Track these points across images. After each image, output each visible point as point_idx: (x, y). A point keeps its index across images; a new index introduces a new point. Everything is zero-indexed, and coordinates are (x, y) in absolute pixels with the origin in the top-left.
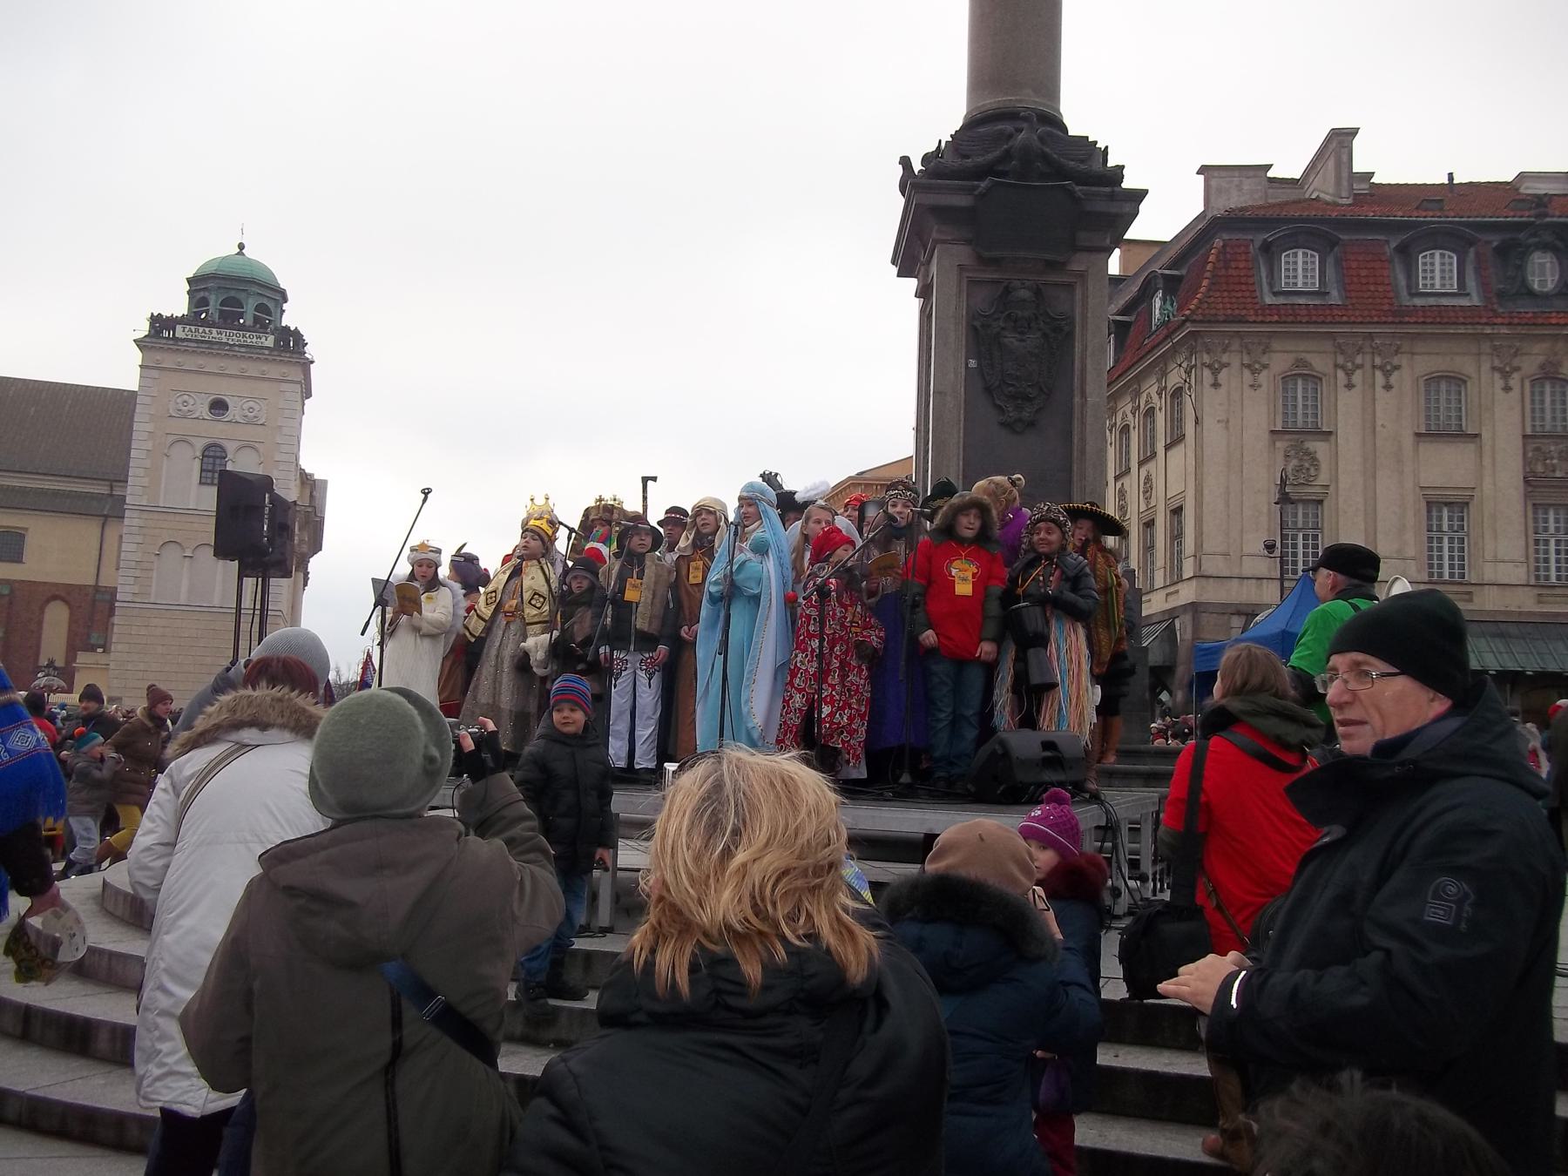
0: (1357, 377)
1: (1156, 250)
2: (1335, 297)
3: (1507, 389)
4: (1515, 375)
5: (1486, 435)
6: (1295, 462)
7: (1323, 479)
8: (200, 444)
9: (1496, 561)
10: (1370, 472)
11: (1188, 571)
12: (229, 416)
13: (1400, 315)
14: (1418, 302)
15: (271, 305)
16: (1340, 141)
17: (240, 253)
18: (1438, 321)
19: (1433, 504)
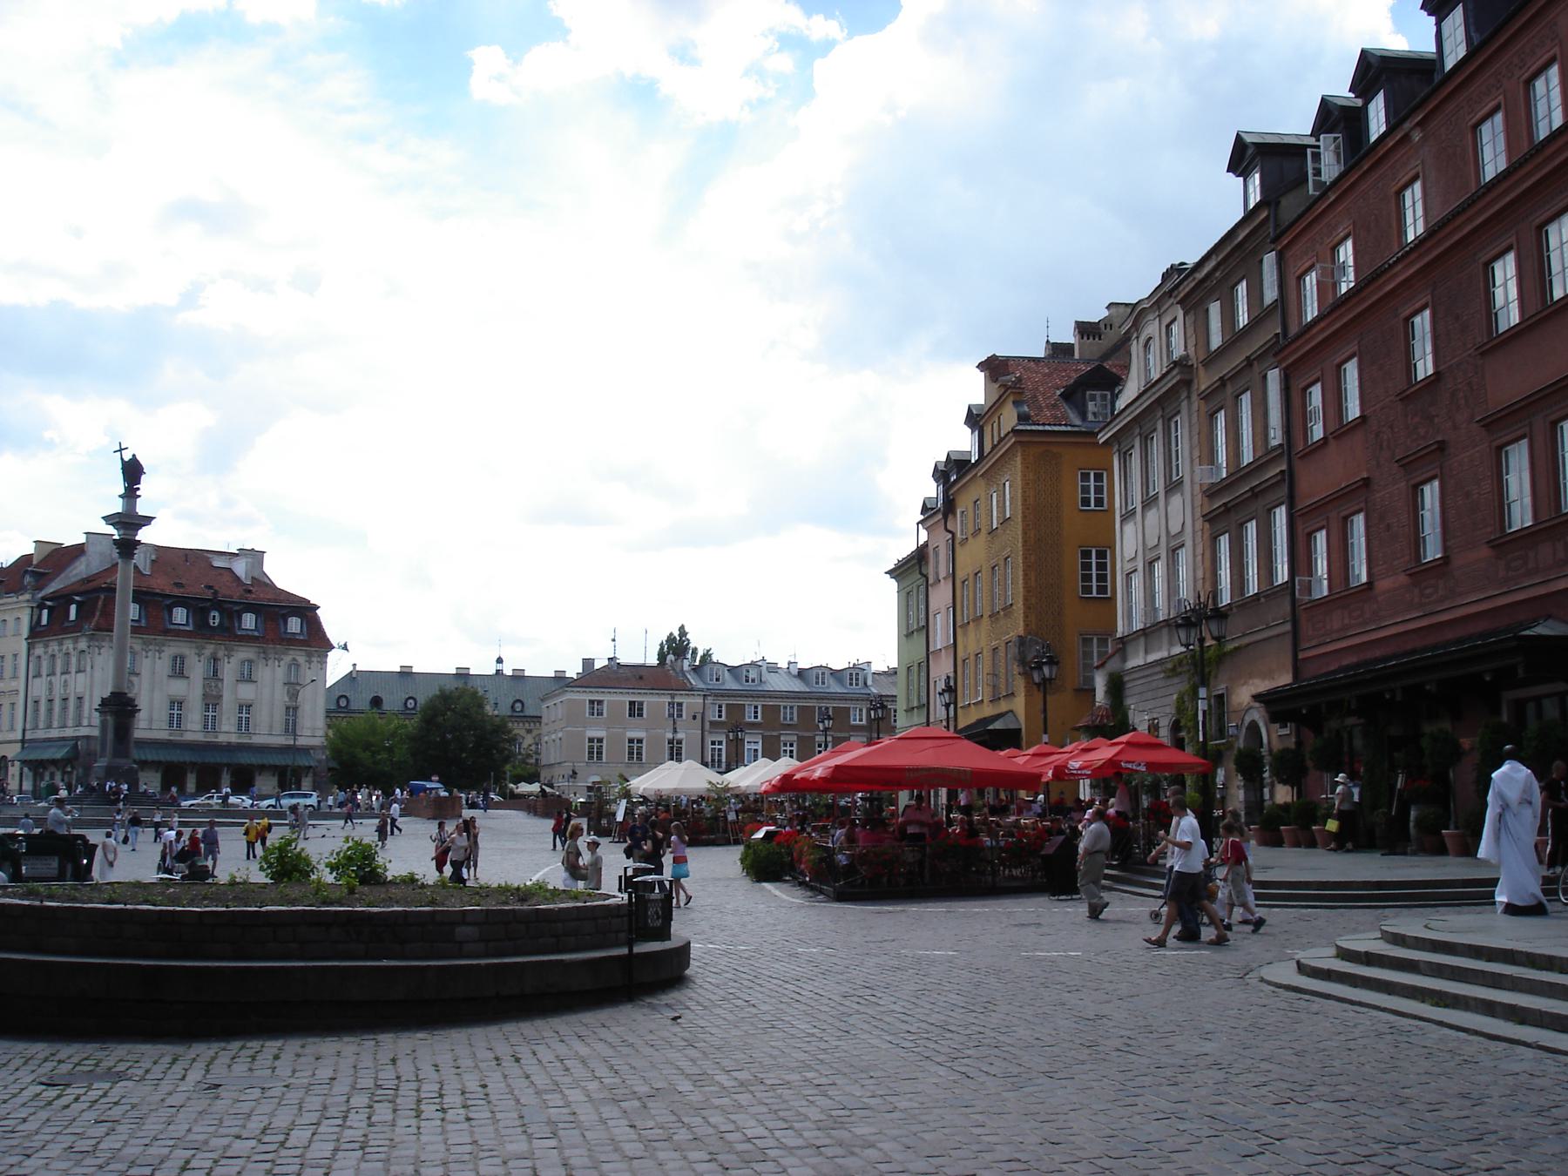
2: (143, 623)
10: (152, 690)
11: (85, 722)
13: (166, 632)
18: (178, 634)
19: (172, 703)
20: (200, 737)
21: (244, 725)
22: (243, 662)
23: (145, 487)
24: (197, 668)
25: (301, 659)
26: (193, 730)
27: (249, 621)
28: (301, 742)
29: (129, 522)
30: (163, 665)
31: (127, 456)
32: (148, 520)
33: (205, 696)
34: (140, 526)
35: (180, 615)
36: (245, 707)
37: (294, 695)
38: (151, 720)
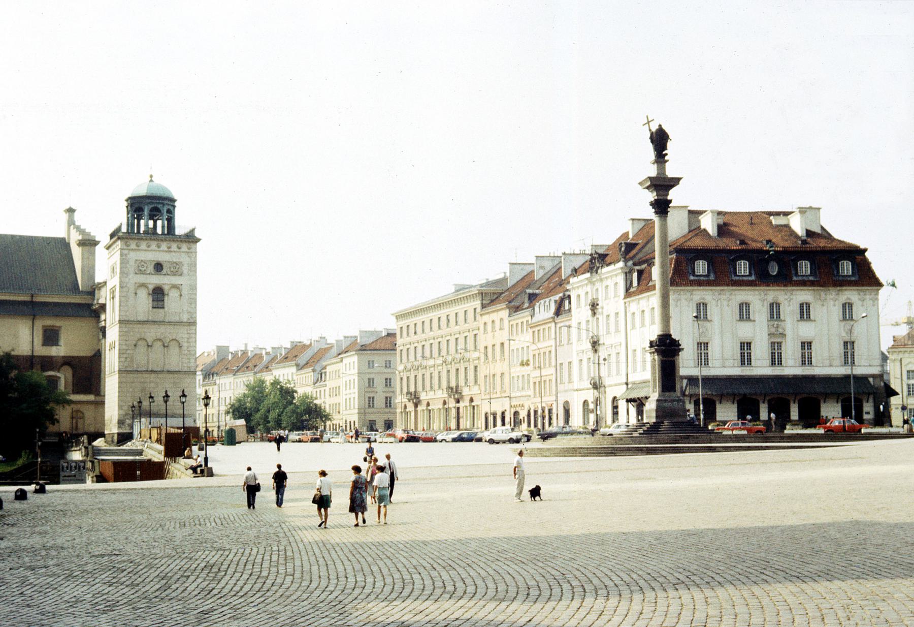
1: (643, 223)
2: (712, 277)
8: (151, 287)
10: (722, 333)
12: (164, 271)
15: (172, 208)
17: (151, 181)
21: (806, 360)
23: (671, 150)
26: (761, 367)
27: (805, 267)
29: (662, 185)
30: (732, 311)
31: (654, 128)
32: (675, 181)
34: (672, 186)
35: (743, 268)
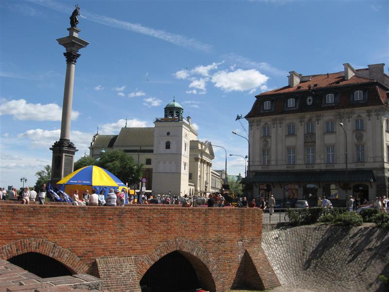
0: (275, 126)
3: (301, 125)
4: (303, 123)
5: (298, 135)
6: (264, 143)
7: (269, 146)
8: (166, 141)
9: (299, 160)
14: (287, 109)
16: (51, 149)
20: (303, 168)
22: (327, 123)
24: (301, 131)
25: (364, 115)
28: (367, 166)
33: (305, 142)
35: (291, 103)
36: (331, 148)
37: (359, 137)
38: (277, 160)
